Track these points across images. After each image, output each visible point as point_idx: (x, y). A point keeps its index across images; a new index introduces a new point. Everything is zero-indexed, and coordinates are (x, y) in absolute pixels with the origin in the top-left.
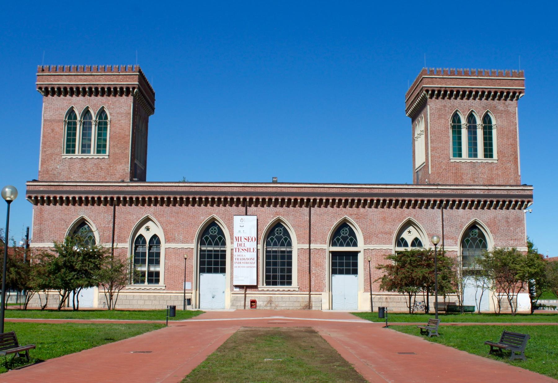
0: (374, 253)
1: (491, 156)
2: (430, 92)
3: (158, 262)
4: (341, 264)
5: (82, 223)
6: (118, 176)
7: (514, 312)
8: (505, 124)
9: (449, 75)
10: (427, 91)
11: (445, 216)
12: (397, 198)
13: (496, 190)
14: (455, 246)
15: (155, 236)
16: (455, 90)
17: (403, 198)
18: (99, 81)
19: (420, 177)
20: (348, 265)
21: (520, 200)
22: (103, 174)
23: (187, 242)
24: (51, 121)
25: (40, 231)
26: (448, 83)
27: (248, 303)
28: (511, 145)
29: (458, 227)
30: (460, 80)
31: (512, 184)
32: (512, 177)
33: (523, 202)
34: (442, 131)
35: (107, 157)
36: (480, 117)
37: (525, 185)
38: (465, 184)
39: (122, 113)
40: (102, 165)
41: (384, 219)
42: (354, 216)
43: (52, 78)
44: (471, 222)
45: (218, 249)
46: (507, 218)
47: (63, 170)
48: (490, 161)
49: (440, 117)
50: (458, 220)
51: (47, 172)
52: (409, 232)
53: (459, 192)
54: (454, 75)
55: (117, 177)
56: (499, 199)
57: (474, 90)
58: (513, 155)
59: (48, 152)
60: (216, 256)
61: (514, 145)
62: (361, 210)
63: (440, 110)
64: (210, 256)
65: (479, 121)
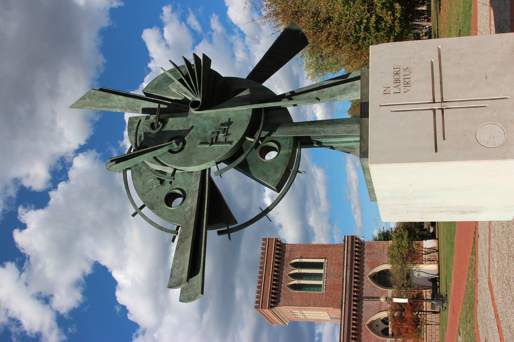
1: (322, 263)
2: (272, 305)
7: (436, 251)
9: (261, 290)
10: (271, 307)
12: (351, 334)
14: (388, 292)
17: (351, 329)
19: (335, 316)
26: (267, 291)
28: (314, 249)
29: (374, 289)
30: (265, 282)
31: (343, 249)
33: (356, 243)
34: (302, 297)
36: (294, 270)
38: (342, 283)
44: (370, 280)
46: (368, 254)
49: (291, 299)
50: (369, 289)
52: (377, 326)
54: (261, 286)
56: (354, 259)
58: (322, 248)
63: (285, 298)
65: (297, 271)
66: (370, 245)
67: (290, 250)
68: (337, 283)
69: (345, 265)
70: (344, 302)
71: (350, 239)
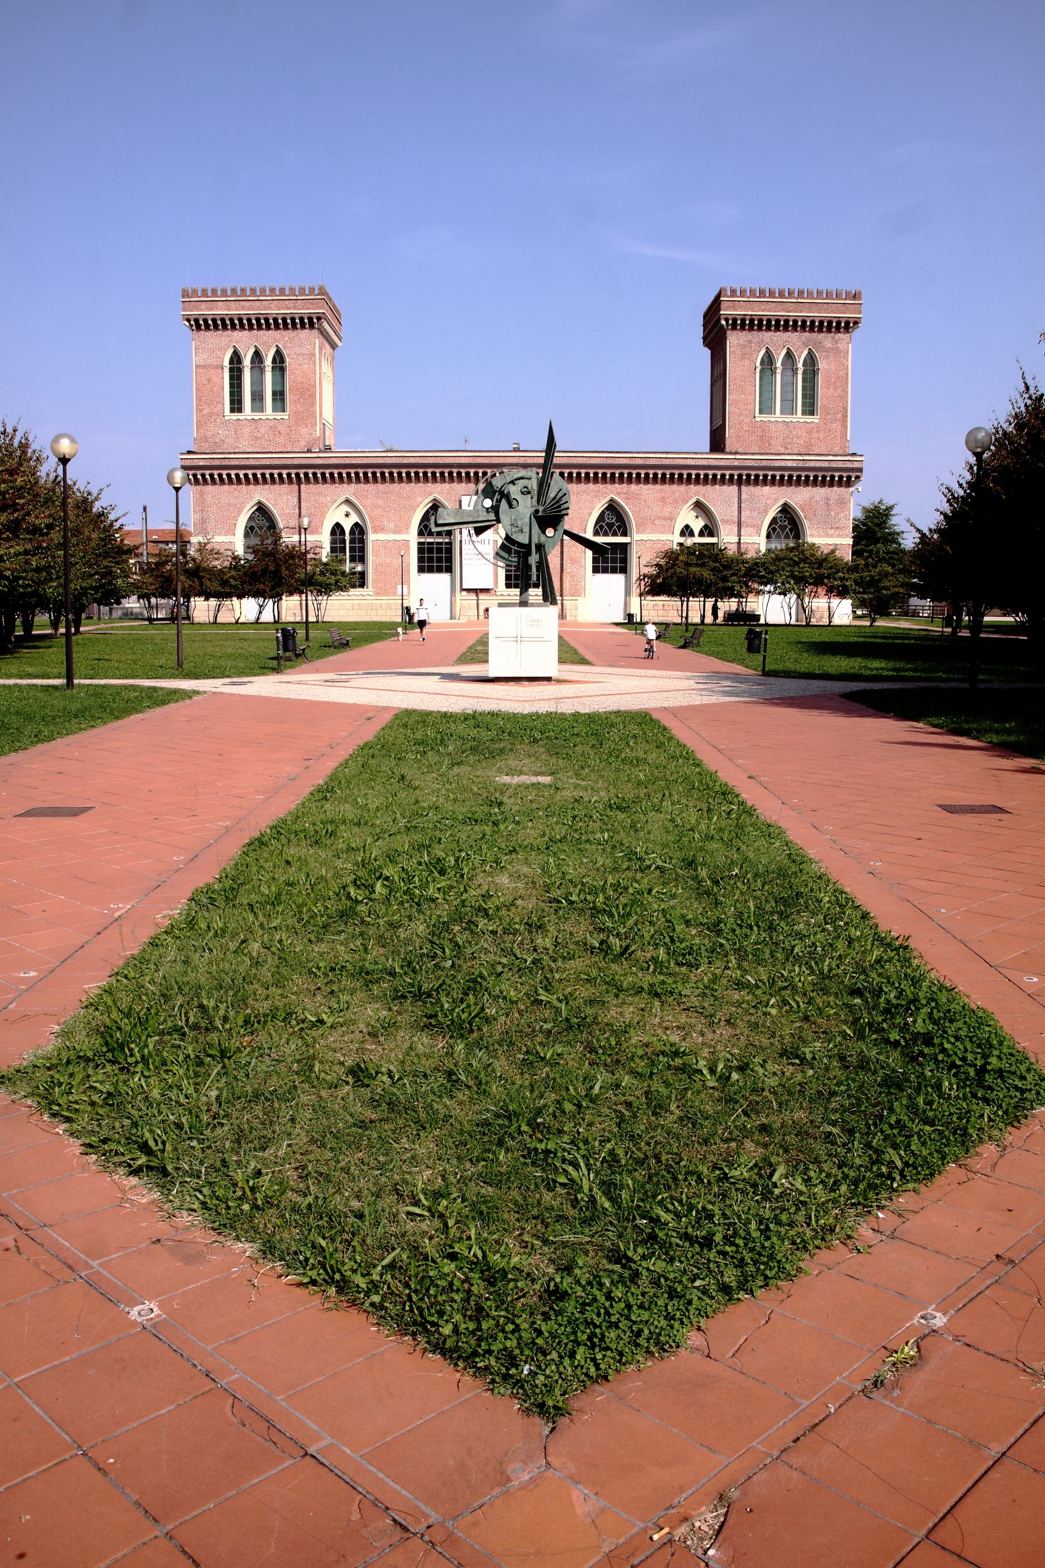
0: (648, 546)
3: (362, 559)
4: (605, 561)
5: (261, 509)
6: (303, 443)
8: (833, 367)
10: (727, 320)
11: (744, 496)
13: (814, 461)
15: (356, 525)
16: (765, 318)
18: (270, 308)
20: (614, 560)
21: (845, 474)
22: (281, 440)
23: (400, 532)
24: (204, 367)
25: (203, 521)
27: (481, 612)
32: (838, 442)
35: (286, 417)
37: (854, 454)
39: (303, 354)
40: (280, 428)
41: (663, 500)
42: (623, 496)
43: (203, 306)
45: (441, 540)
46: (828, 499)
47: (227, 436)
48: (809, 421)
51: (206, 439)
53: (765, 464)
54: (764, 297)
55: (302, 445)
57: (791, 319)
59: (205, 412)
60: (439, 550)
61: (844, 398)
62: (633, 487)
63: (744, 346)
64: (430, 550)
66: (843, 503)
67: (838, 349)
68: (773, 442)
69: (806, 458)
70: (738, 457)
71: (856, 465)
